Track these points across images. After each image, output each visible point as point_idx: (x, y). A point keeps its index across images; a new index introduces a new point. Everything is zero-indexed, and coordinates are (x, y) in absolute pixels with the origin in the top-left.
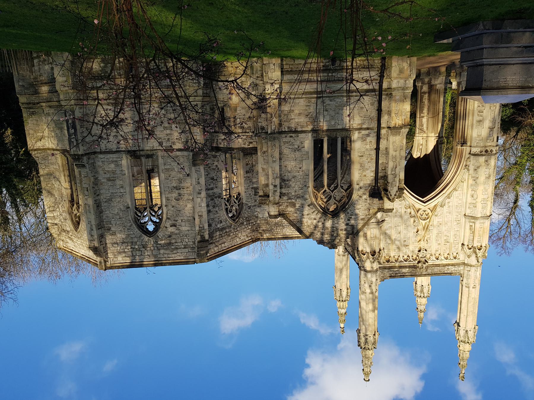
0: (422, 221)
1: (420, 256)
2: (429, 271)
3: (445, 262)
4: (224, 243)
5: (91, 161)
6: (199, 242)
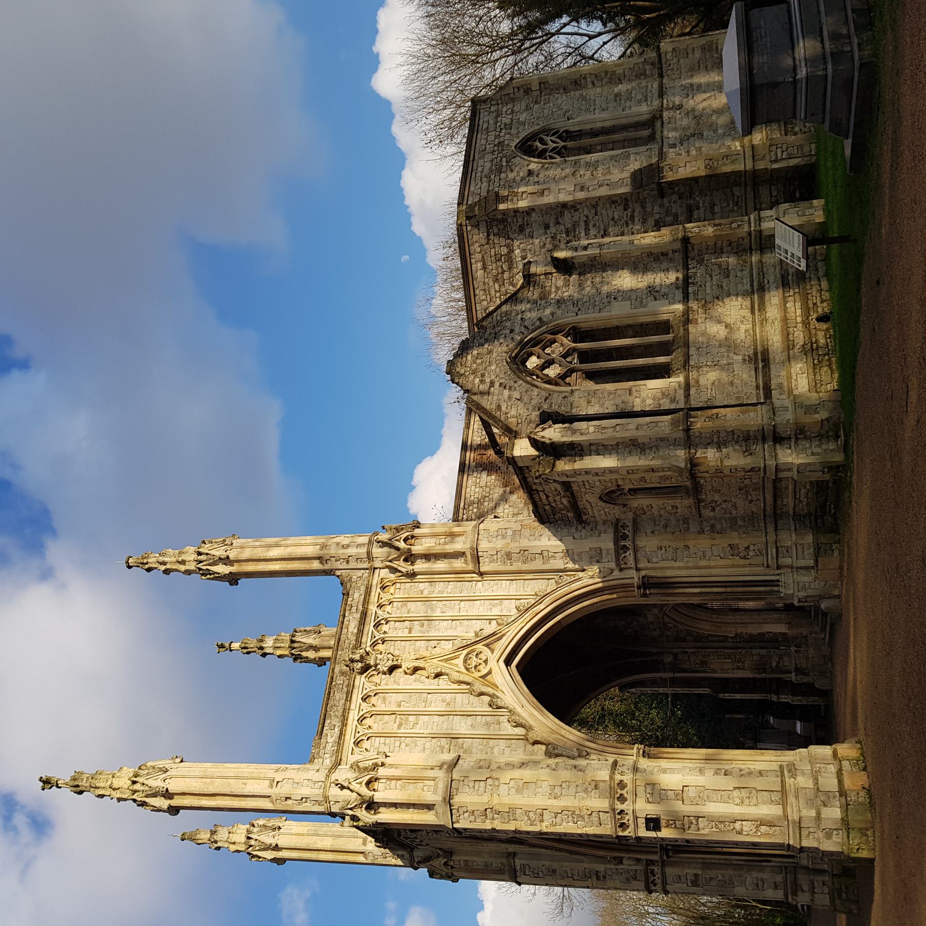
0: (462, 657)
1: (379, 656)
2: (340, 680)
3: (353, 716)
4: (484, 268)
5: (648, 67)
6: (497, 194)
